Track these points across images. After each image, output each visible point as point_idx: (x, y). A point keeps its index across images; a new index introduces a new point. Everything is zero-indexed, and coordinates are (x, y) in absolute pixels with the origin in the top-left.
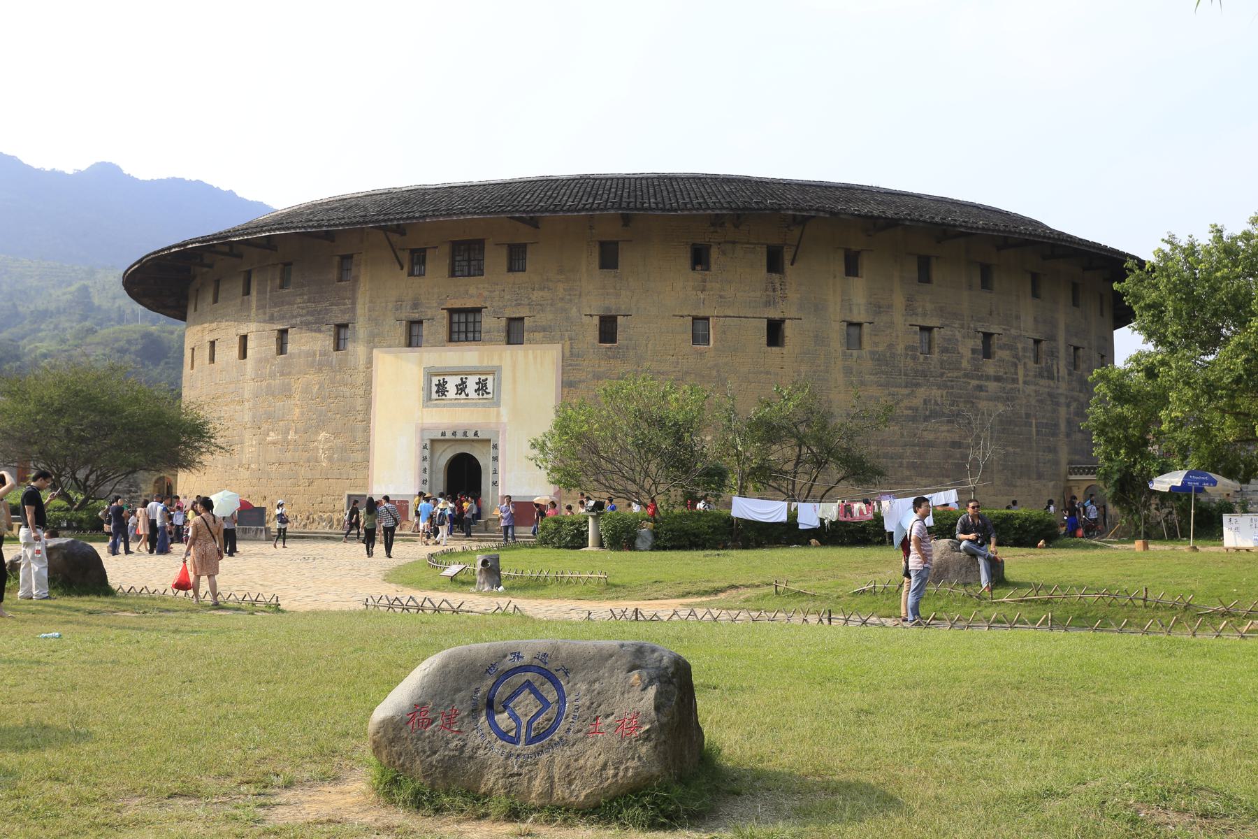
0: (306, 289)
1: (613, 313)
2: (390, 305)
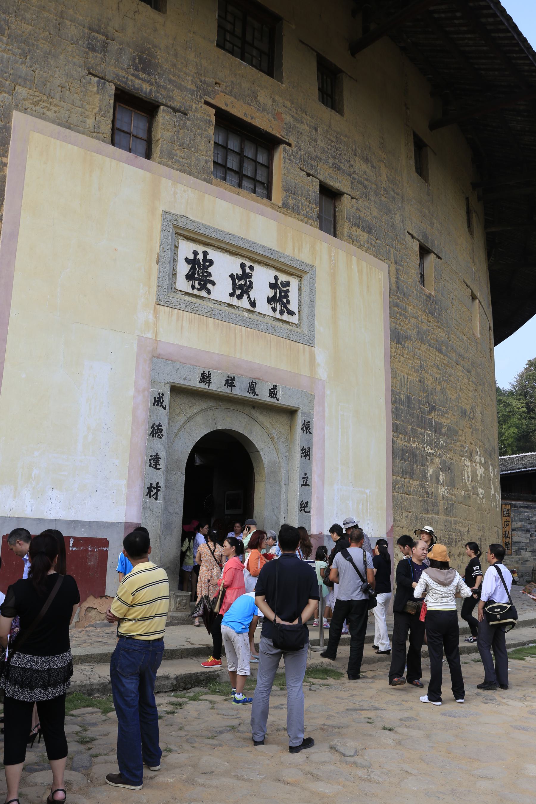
2: (72, 30)
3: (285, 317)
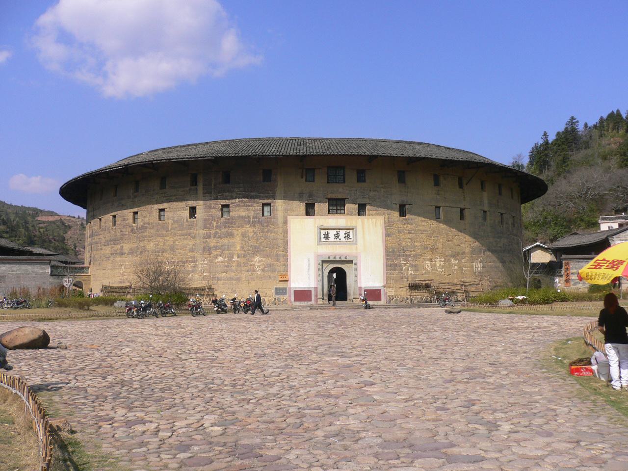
0: (241, 185)
1: (405, 203)
3: (349, 240)
